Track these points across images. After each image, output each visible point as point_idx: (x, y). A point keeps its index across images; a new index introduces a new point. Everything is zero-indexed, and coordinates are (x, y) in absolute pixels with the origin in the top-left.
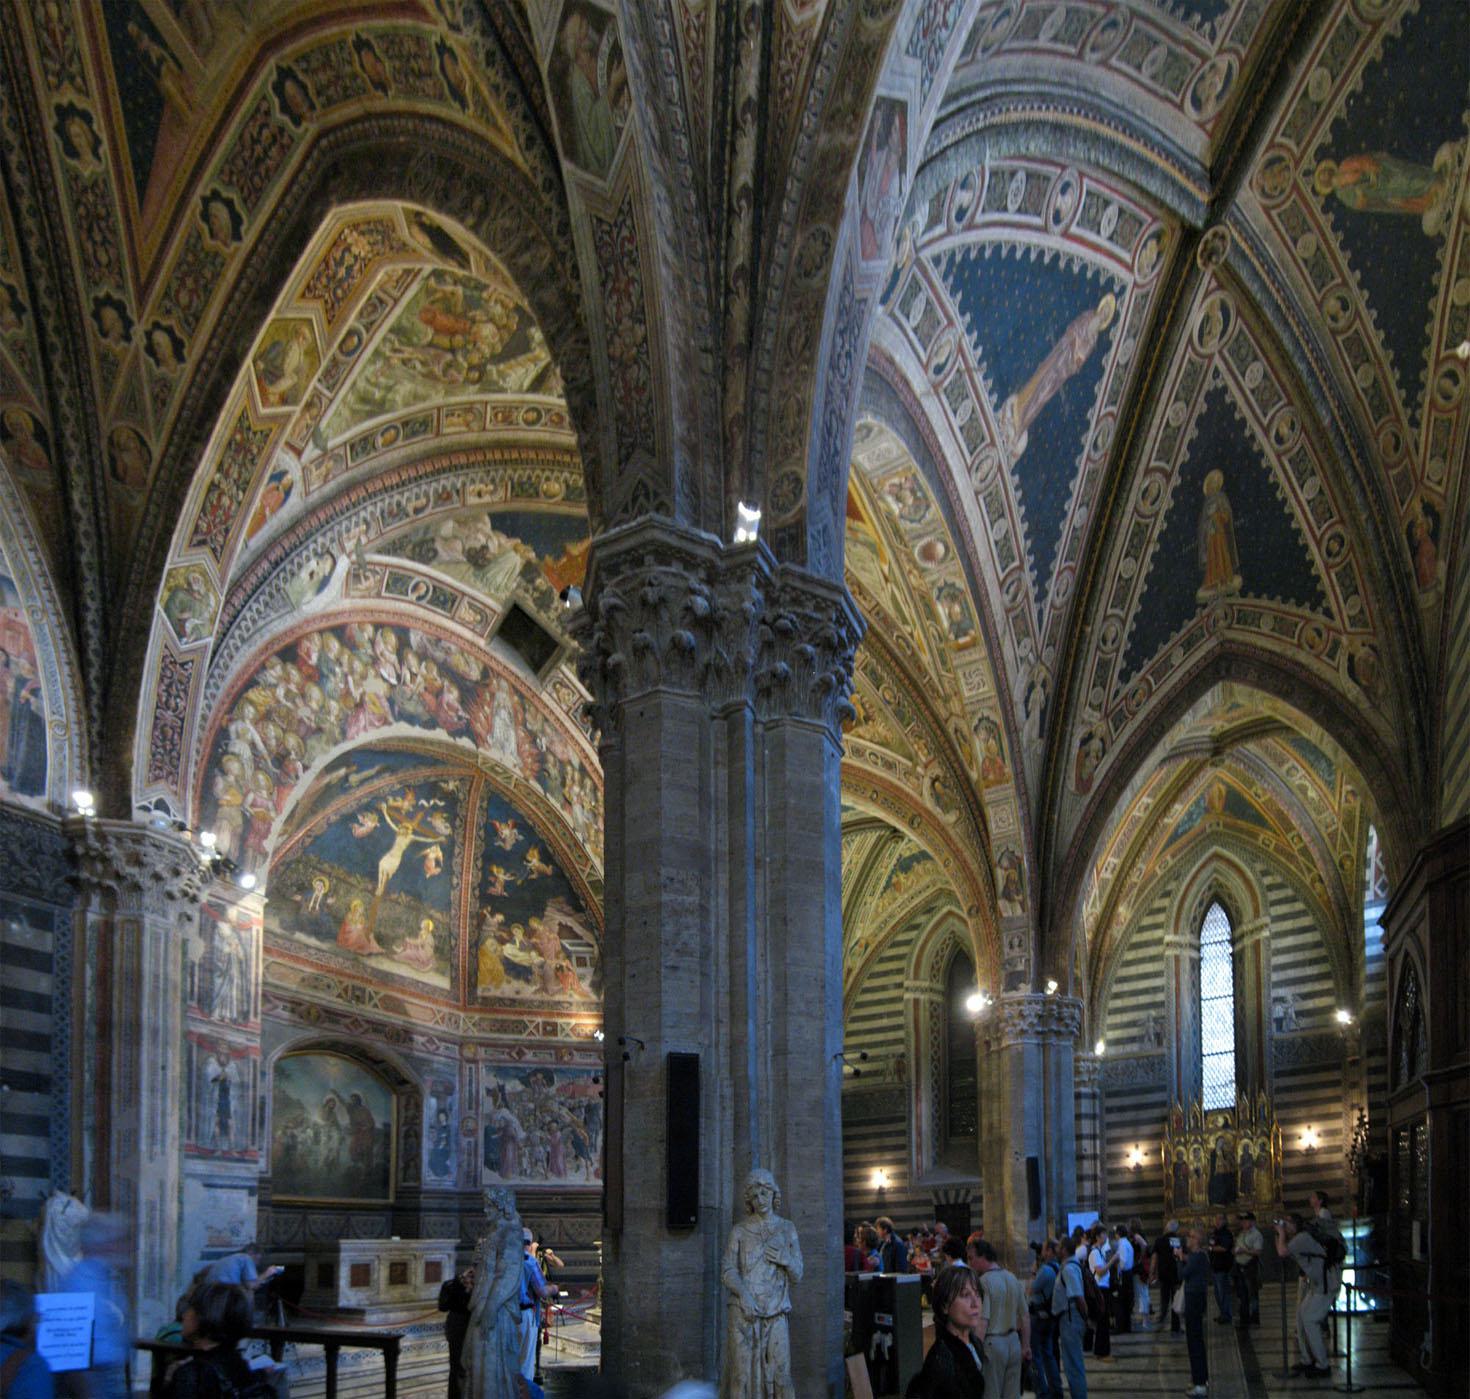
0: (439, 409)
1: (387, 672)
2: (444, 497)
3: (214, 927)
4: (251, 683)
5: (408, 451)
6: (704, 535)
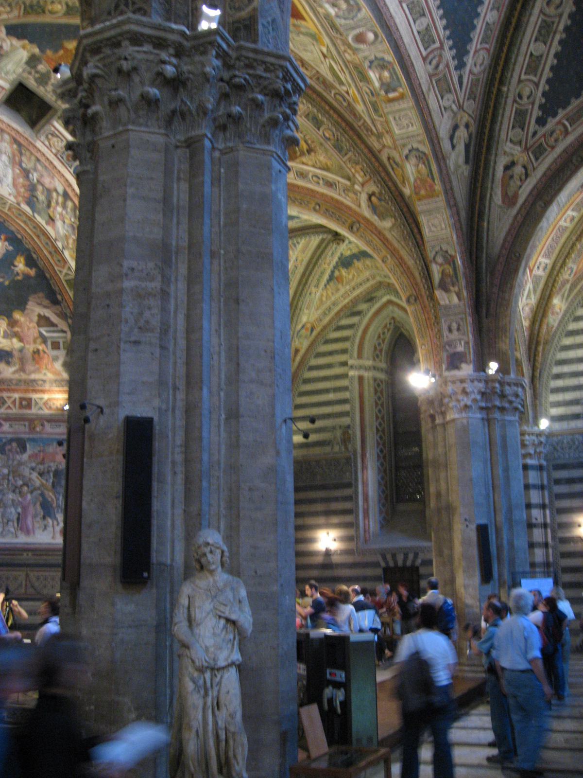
6: (174, 26)
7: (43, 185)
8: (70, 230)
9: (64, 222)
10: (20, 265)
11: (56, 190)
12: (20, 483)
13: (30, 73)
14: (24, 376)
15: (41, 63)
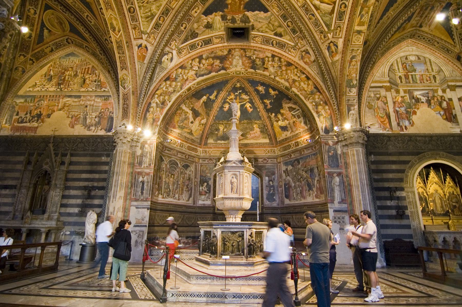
0: (166, 4)
1: (196, 68)
2: (189, 20)
3: (144, 146)
4: (158, 89)
5: (170, 18)
7: (259, 58)
8: (278, 68)
9: (274, 67)
10: (272, 92)
11: (267, 57)
12: (300, 177)
13: (227, 22)
14: (293, 134)
15: (227, 16)
